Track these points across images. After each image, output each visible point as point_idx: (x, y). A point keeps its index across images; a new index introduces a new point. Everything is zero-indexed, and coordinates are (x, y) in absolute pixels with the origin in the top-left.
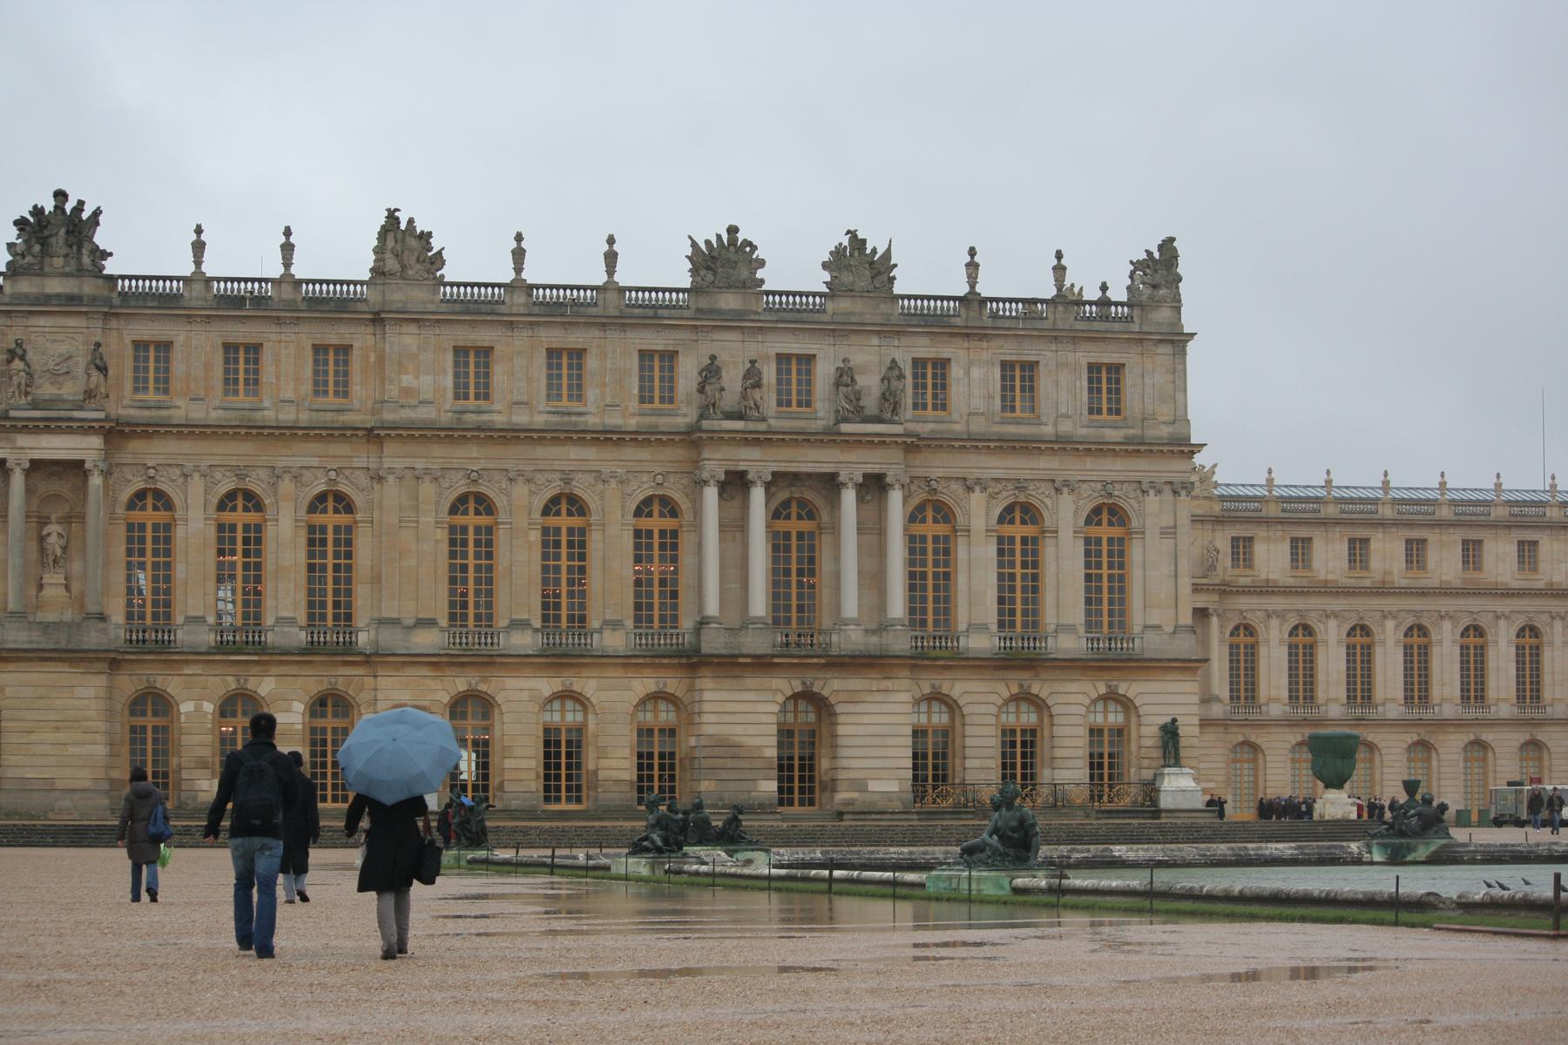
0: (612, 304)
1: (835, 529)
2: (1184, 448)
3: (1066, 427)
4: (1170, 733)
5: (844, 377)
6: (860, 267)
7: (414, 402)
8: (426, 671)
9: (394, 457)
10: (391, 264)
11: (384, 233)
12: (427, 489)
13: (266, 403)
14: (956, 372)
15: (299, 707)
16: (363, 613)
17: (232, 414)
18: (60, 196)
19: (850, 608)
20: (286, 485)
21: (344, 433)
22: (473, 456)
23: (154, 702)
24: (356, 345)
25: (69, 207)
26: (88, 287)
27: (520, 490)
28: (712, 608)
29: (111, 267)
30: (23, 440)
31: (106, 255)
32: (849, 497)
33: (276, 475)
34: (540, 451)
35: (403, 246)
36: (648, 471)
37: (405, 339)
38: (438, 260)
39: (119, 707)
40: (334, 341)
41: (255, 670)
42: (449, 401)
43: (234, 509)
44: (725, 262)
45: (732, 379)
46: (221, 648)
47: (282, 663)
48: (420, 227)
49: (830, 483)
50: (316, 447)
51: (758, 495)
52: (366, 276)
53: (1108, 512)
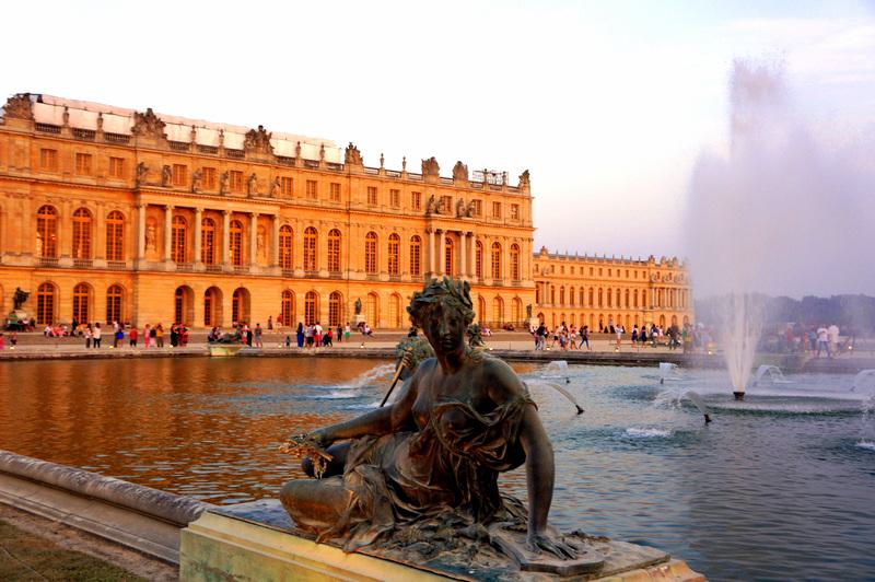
0: (406, 178)
1: (459, 249)
2: (531, 229)
3: (507, 222)
4: (529, 308)
5: (460, 204)
6: (460, 169)
9: (354, 220)
10: (351, 159)
11: (347, 150)
14: (483, 204)
15: (328, 296)
16: (343, 267)
18: (261, 127)
19: (464, 271)
21: (338, 211)
23: (288, 294)
26: (270, 158)
27: (384, 232)
28: (433, 269)
30: (258, 207)
32: (463, 238)
33: (321, 222)
34: (390, 220)
35: (352, 152)
36: (416, 227)
37: (355, 183)
38: (361, 159)
40: (336, 182)
42: (367, 204)
44: (430, 165)
45: (437, 198)
46: (306, 277)
49: (458, 234)
50: (332, 215)
51: (443, 236)
53: (515, 246)
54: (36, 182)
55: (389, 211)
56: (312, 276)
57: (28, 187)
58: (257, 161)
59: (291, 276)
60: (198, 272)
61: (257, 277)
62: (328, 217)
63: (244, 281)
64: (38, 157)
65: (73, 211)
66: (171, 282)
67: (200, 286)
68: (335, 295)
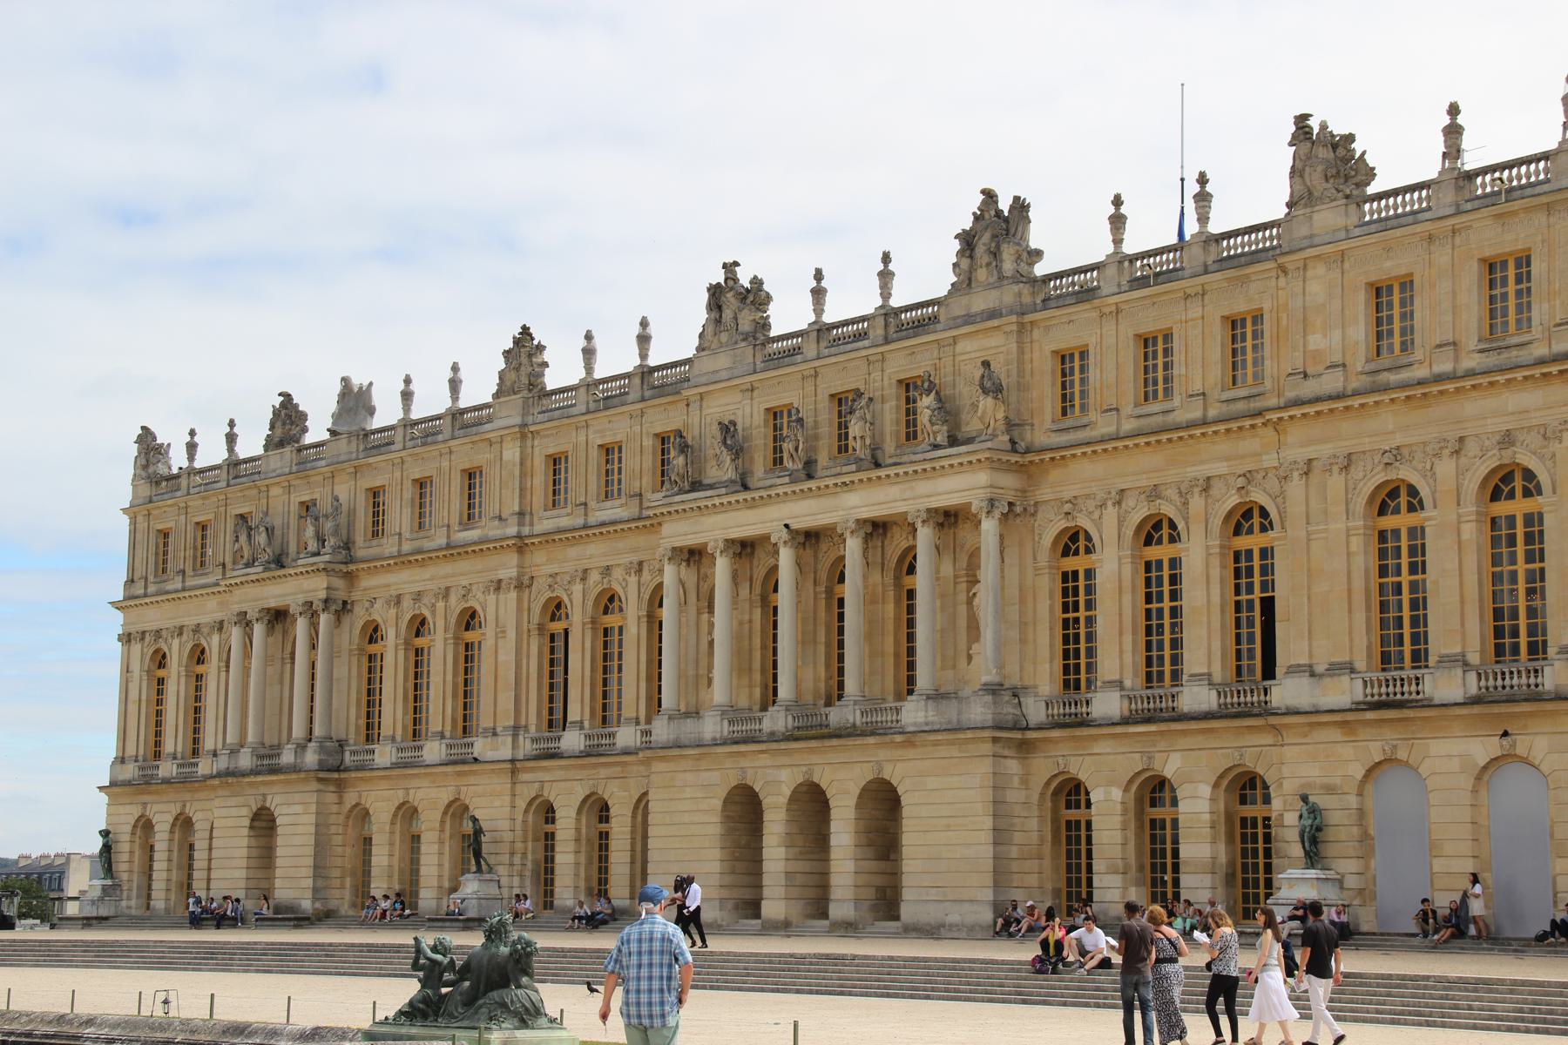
7: (1320, 368)
8: (1336, 734)
12: (1336, 482)
13: (1177, 401)
15: (1205, 790)
17: (1143, 421)
18: (990, 196)
20: (1197, 503)
22: (1387, 426)
24: (1266, 306)
25: (1004, 205)
27: (1446, 468)
29: (1040, 270)
30: (923, 487)
31: (1037, 254)
35: (1326, 161)
37: (1318, 283)
39: (1035, 797)
41: (1162, 745)
43: (1160, 542)
47: (1184, 733)
48: (1338, 129)
50: (1224, 446)
52: (1280, 212)
54: (521, 545)
55: (1471, 362)
56: (1154, 714)
57: (513, 558)
58: (969, 319)
59: (1084, 723)
60: (773, 737)
61: (911, 738)
62: (1217, 459)
63: (882, 754)
64: (540, 480)
65: (590, 603)
66: (713, 777)
67: (777, 782)
68: (1247, 786)
